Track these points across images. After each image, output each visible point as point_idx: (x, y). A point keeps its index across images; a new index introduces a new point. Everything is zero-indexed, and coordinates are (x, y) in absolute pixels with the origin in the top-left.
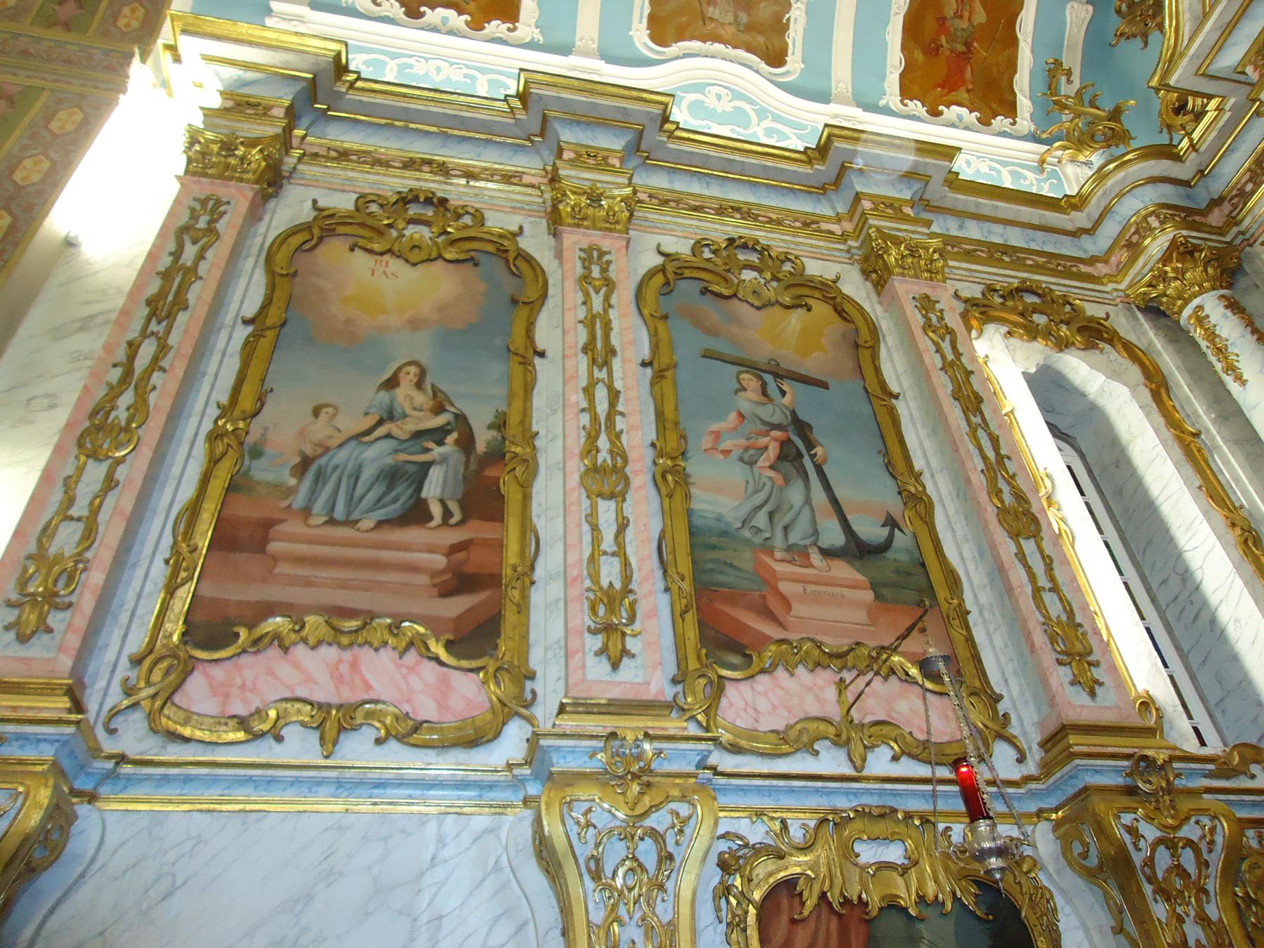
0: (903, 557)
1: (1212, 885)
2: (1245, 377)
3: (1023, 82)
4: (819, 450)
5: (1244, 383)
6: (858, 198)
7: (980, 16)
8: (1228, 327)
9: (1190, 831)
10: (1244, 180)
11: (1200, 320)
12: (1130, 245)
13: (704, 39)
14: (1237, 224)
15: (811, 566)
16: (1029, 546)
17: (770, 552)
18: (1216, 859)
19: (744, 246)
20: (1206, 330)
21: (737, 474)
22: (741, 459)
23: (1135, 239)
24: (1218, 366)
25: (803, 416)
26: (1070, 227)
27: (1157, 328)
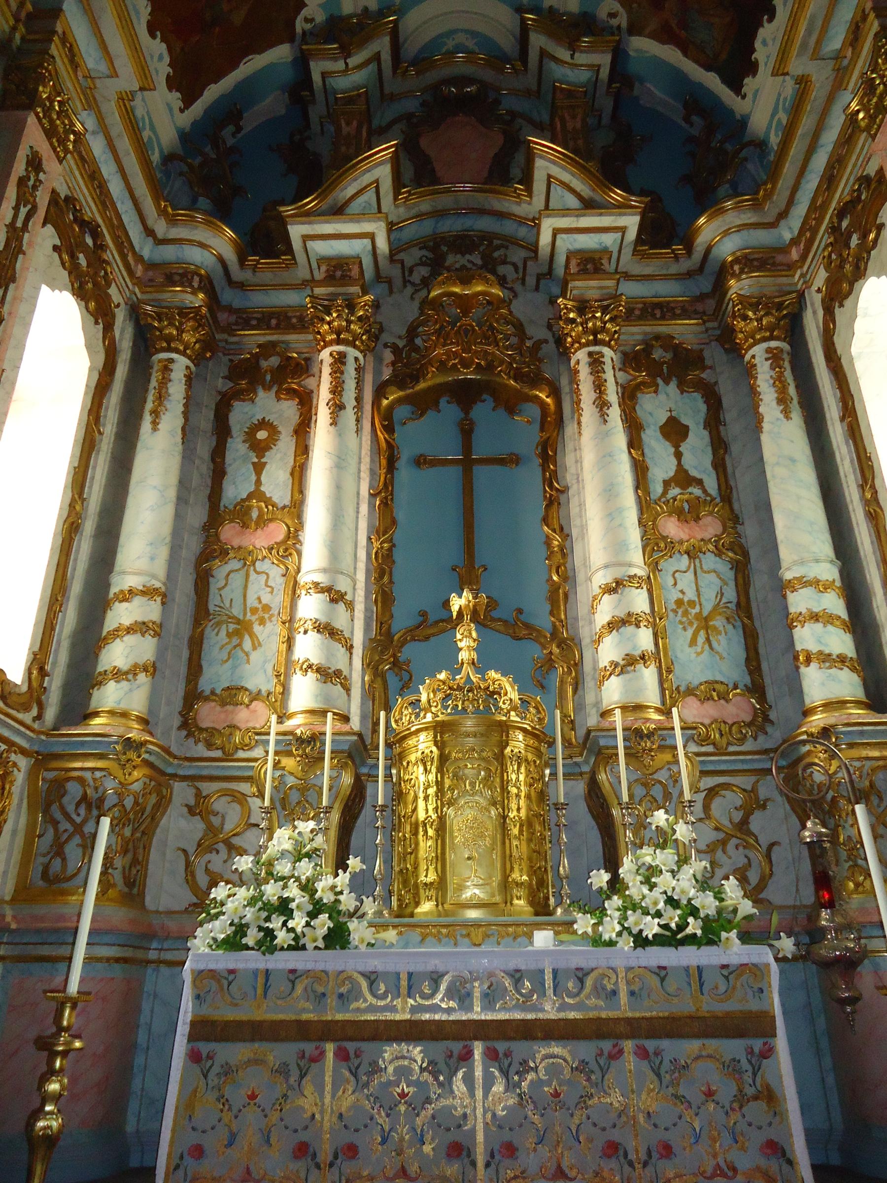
2: (159, 426)
3: (212, 93)
7: (238, 18)
8: (177, 390)
10: (255, 315)
11: (166, 368)
14: (229, 335)
20: (163, 378)
24: (149, 405)
26: (150, 223)
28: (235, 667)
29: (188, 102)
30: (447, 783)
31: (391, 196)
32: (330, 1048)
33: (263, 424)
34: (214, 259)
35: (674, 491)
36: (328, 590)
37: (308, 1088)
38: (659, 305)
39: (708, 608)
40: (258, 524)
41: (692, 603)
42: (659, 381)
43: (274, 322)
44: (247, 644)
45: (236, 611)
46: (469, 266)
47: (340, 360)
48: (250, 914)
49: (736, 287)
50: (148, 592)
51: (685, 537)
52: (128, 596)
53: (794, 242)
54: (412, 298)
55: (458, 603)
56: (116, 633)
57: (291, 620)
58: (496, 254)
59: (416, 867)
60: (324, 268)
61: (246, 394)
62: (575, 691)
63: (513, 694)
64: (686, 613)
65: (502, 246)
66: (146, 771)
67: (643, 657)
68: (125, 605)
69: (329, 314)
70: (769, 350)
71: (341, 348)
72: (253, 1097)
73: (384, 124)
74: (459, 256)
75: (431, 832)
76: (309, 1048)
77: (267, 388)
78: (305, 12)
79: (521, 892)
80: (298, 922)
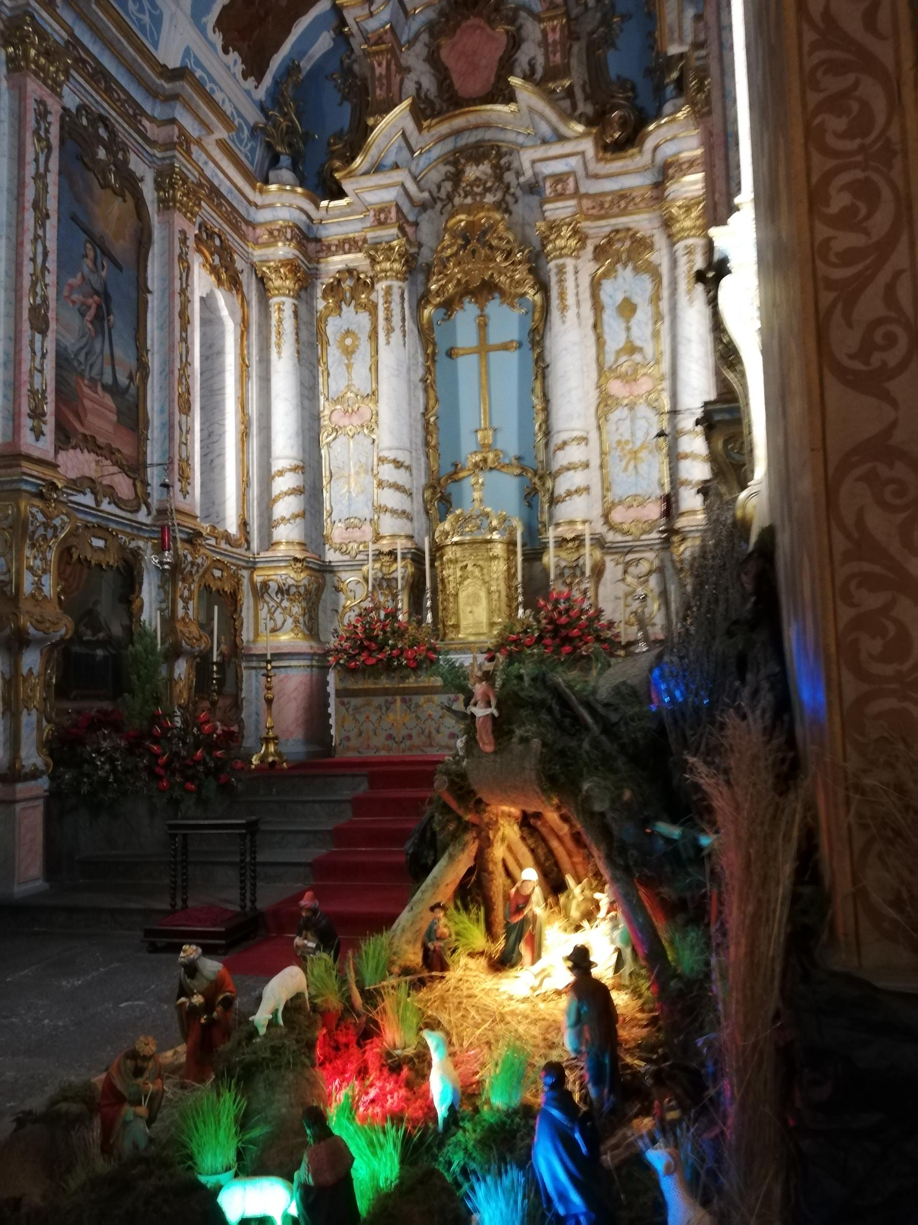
0: (131, 399)
1: (196, 578)
3: (276, 62)
4: (111, 317)
5: (280, 358)
6: (173, 121)
8: (289, 325)
9: (199, 561)
12: (271, 233)
15: (96, 392)
16: (184, 417)
17: (83, 378)
18: (201, 571)
19: (106, 127)
21: (75, 321)
22: (79, 310)
23: (276, 233)
24: (274, 339)
25: (110, 291)
27: (258, 290)
28: (350, 505)
29: (259, 79)
31: (416, 132)
32: (398, 698)
33: (348, 333)
34: (298, 212)
39: (638, 444)
41: (627, 442)
43: (347, 246)
46: (483, 177)
50: (294, 469)
51: (627, 394)
52: (281, 473)
54: (442, 213)
56: (279, 497)
58: (503, 162)
62: (550, 507)
65: (506, 154)
66: (308, 572)
68: (281, 479)
72: (368, 718)
73: (412, 34)
74: (474, 167)
75: (451, 599)
76: (390, 698)
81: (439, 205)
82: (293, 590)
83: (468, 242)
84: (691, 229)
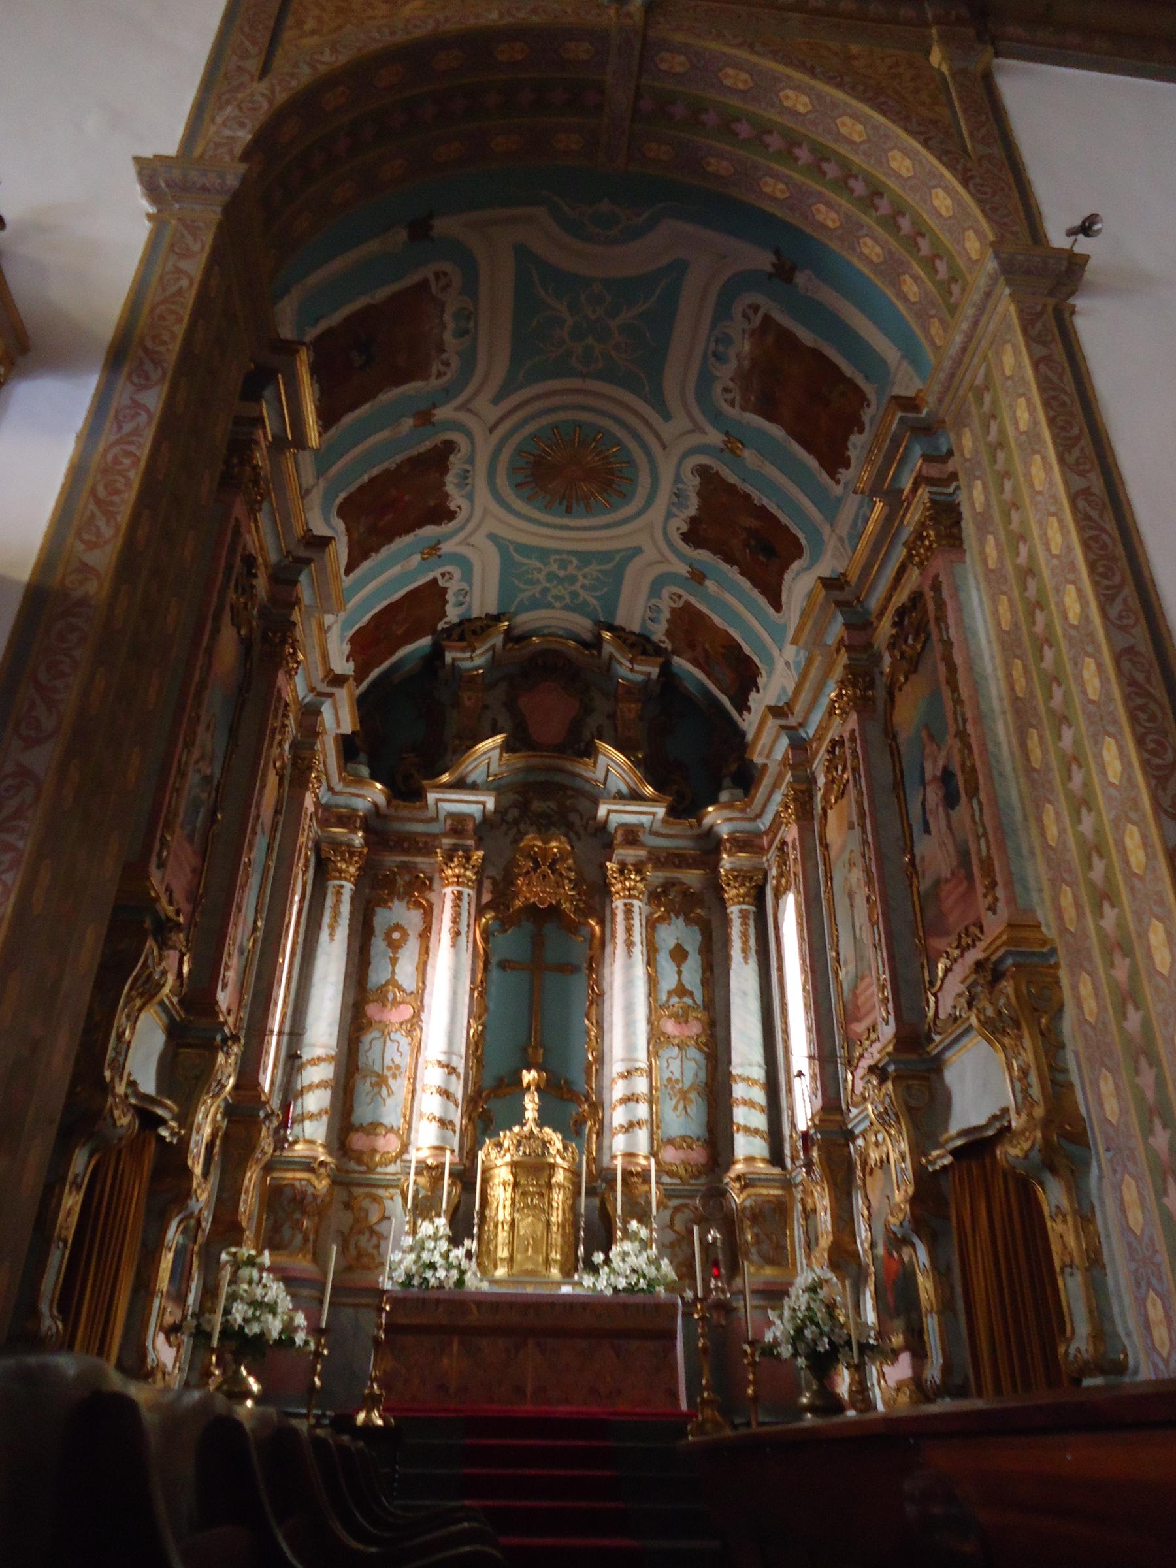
3: (375, 673)
5: (332, 940)
7: (399, 632)
8: (345, 908)
11: (339, 893)
13: (348, 530)
24: (326, 919)
30: (517, 1198)
33: (398, 927)
35: (674, 1000)
36: (448, 1066)
37: (445, 1361)
38: (678, 856)
39: (687, 1084)
40: (393, 1005)
41: (677, 1081)
42: (672, 915)
44: (384, 1091)
45: (377, 1068)
47: (459, 896)
48: (414, 1269)
49: (726, 861)
51: (677, 1033)
53: (766, 833)
55: (529, 1076)
56: (311, 1087)
57: (415, 1079)
58: (568, 803)
59: (496, 1247)
60: (449, 822)
61: (384, 903)
62: (597, 1138)
63: (559, 1145)
64: (673, 1088)
67: (638, 1123)
68: (315, 1068)
69: (452, 861)
70: (741, 911)
71: (459, 888)
77: (400, 898)
78: (446, 620)
79: (557, 1266)
80: (441, 1274)
81: (504, 827)
82: (309, 1199)
83: (537, 866)
84: (744, 896)
